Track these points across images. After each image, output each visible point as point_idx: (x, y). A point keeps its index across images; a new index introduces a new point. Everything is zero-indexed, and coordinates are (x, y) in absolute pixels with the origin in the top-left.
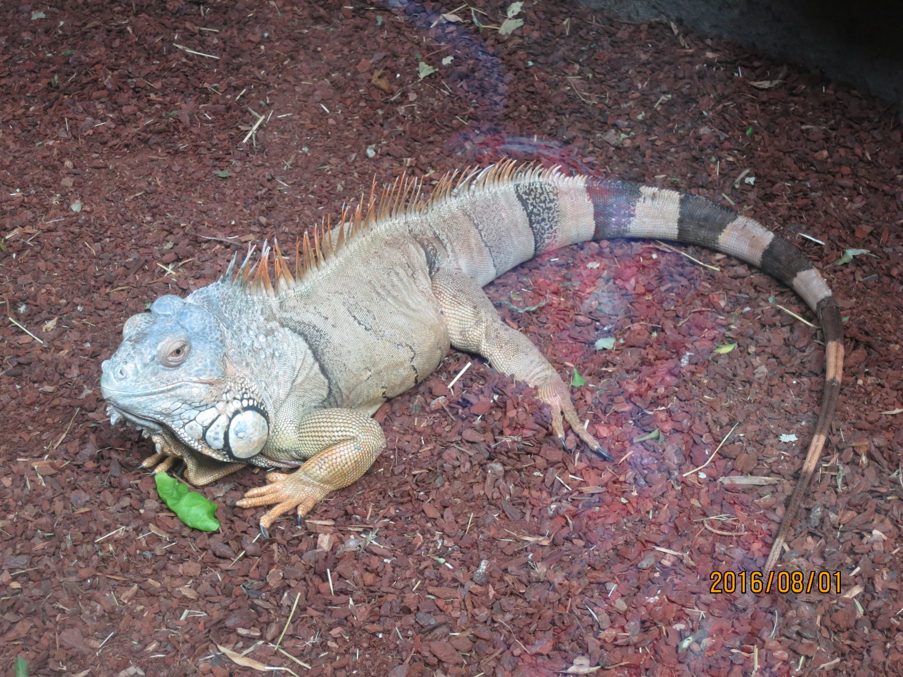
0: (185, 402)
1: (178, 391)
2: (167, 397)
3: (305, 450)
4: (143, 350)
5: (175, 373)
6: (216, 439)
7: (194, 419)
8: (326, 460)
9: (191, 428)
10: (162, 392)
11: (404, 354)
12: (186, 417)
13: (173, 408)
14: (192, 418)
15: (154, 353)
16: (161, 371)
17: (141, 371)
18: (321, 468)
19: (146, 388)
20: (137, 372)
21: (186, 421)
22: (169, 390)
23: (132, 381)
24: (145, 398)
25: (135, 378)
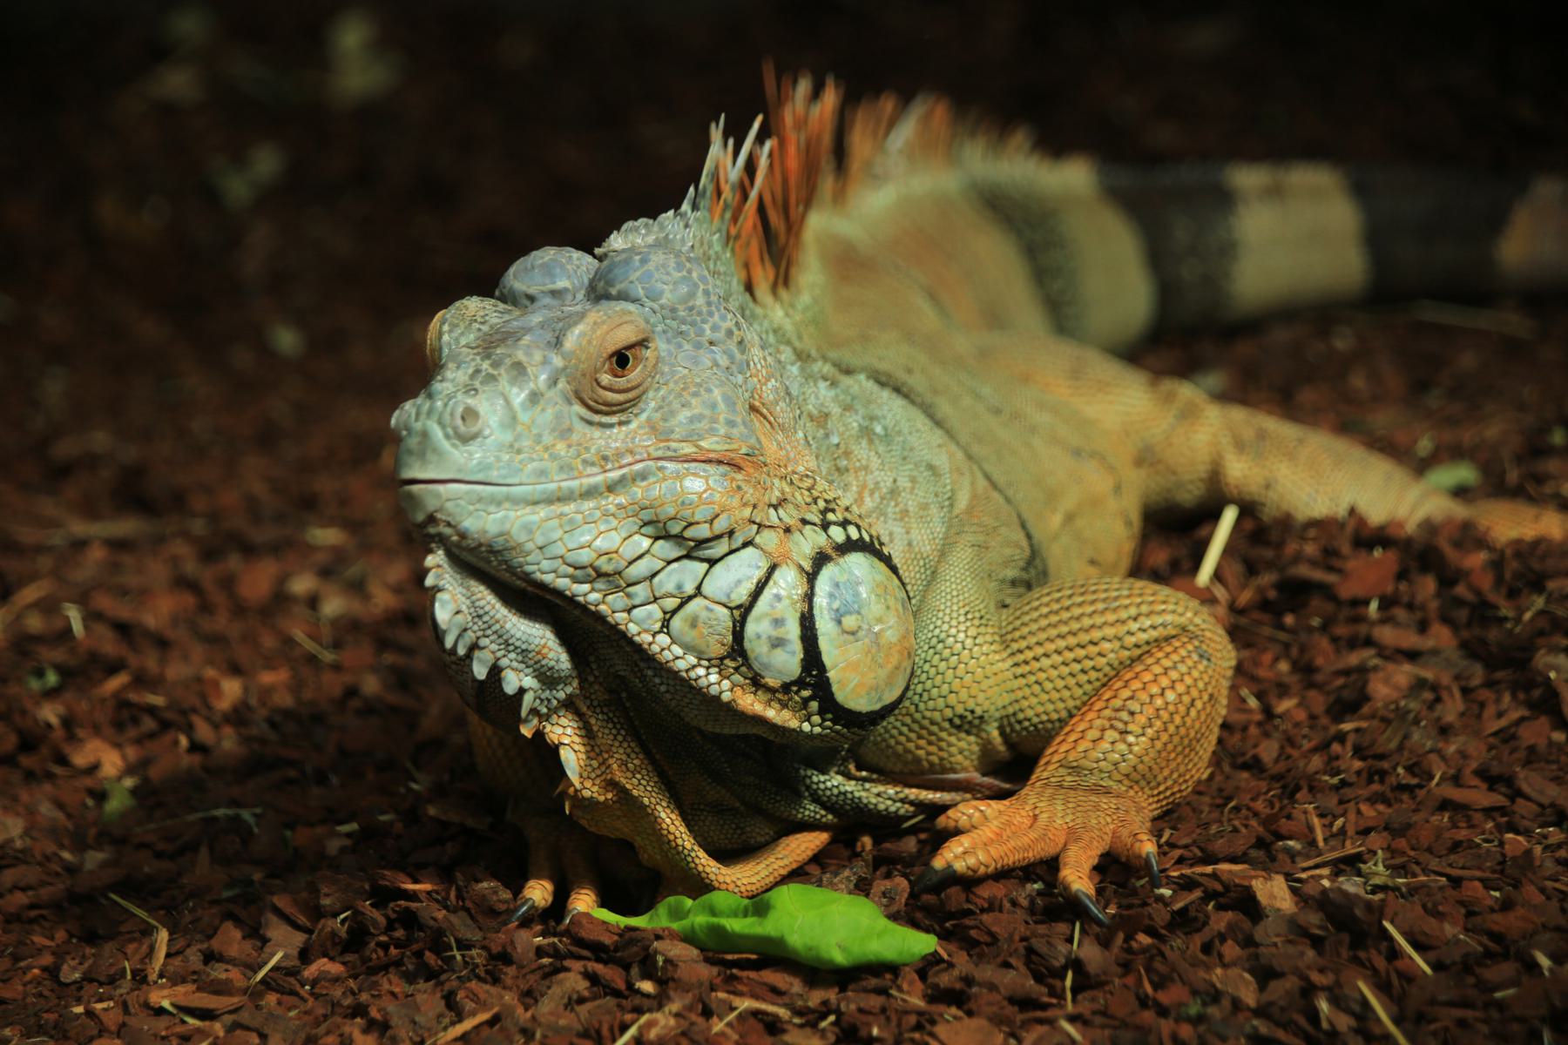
0: (663, 535)
1: (638, 491)
2: (606, 514)
3: (1037, 707)
4: (520, 356)
5: (614, 438)
6: (778, 643)
7: (698, 591)
8: (1135, 706)
9: (694, 623)
10: (589, 493)
11: (1201, 485)
12: (670, 587)
13: (629, 551)
14: (689, 589)
15: (558, 362)
16: (580, 426)
17: (524, 417)
18: (1125, 732)
19: (542, 473)
20: (514, 418)
21: (671, 603)
22: (611, 488)
23: (501, 447)
24: (543, 512)
25: (508, 437)
